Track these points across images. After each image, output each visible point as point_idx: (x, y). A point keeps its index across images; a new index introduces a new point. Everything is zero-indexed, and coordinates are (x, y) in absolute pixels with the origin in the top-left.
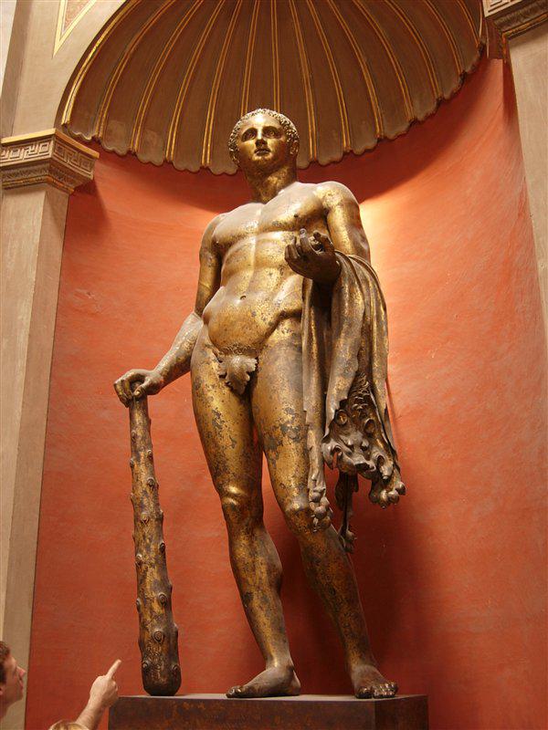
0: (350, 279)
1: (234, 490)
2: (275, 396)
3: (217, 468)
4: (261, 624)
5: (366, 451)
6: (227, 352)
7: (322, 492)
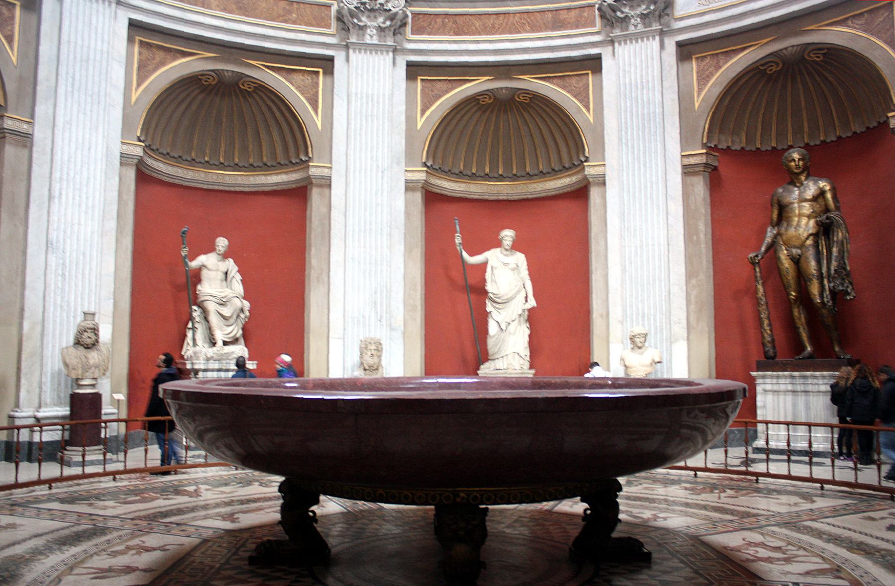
1: (793, 294)
5: (842, 285)
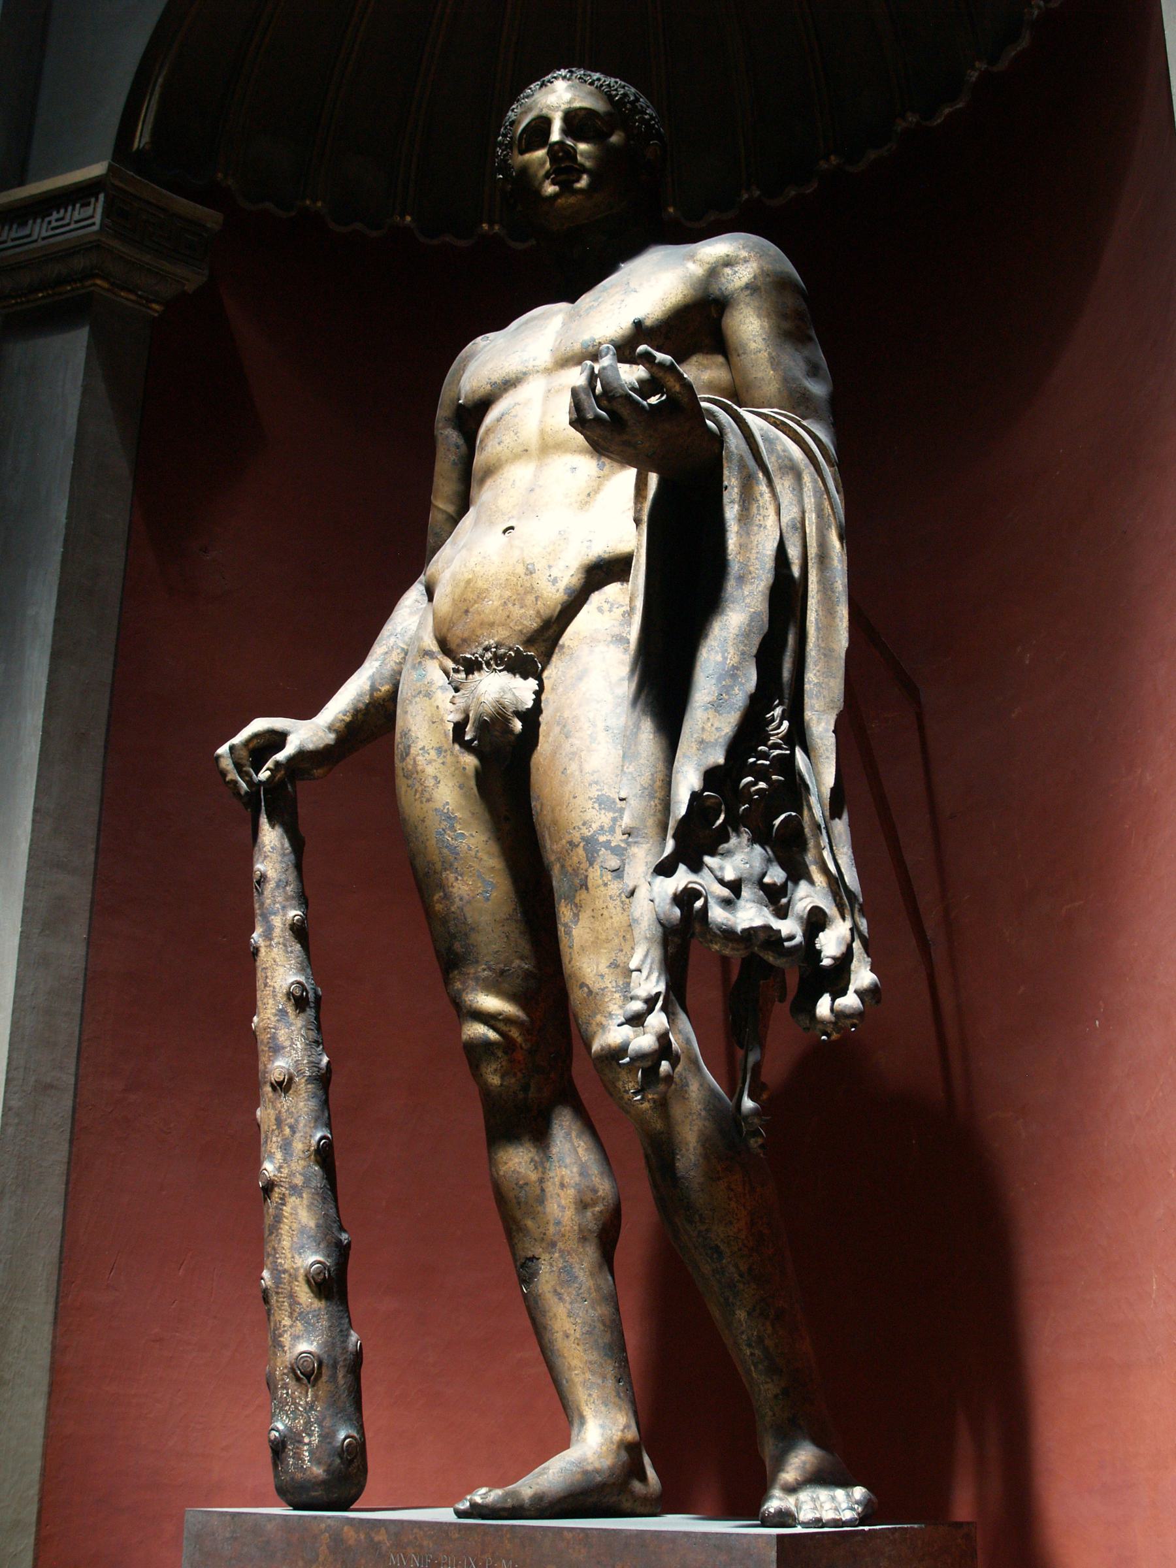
0: (742, 466)
2: (573, 767)
3: (450, 949)
4: (559, 1336)
5: (776, 899)
6: (472, 667)
7: (651, 1002)
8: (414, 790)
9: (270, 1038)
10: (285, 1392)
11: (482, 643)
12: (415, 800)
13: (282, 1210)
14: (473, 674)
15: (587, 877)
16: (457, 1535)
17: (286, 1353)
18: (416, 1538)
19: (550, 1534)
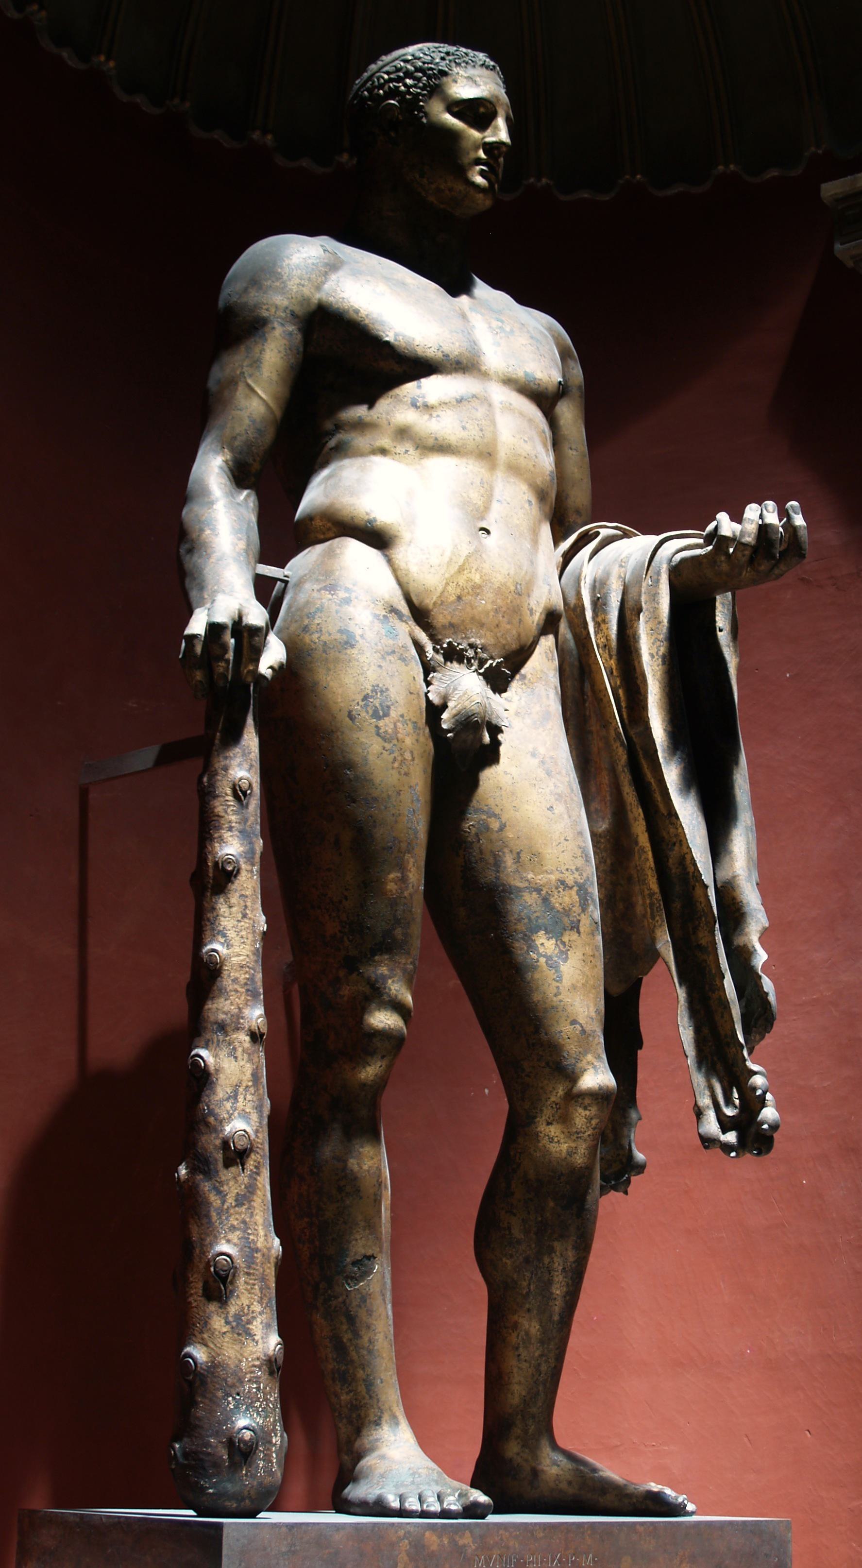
6: (453, 655)
8: (392, 756)
9: (248, 979)
10: (255, 1386)
11: (469, 638)
12: (393, 768)
13: (256, 1179)
14: (451, 662)
15: (579, 921)
16: (542, 1534)
17: (257, 1343)
18: (502, 1539)
19: (625, 1529)
